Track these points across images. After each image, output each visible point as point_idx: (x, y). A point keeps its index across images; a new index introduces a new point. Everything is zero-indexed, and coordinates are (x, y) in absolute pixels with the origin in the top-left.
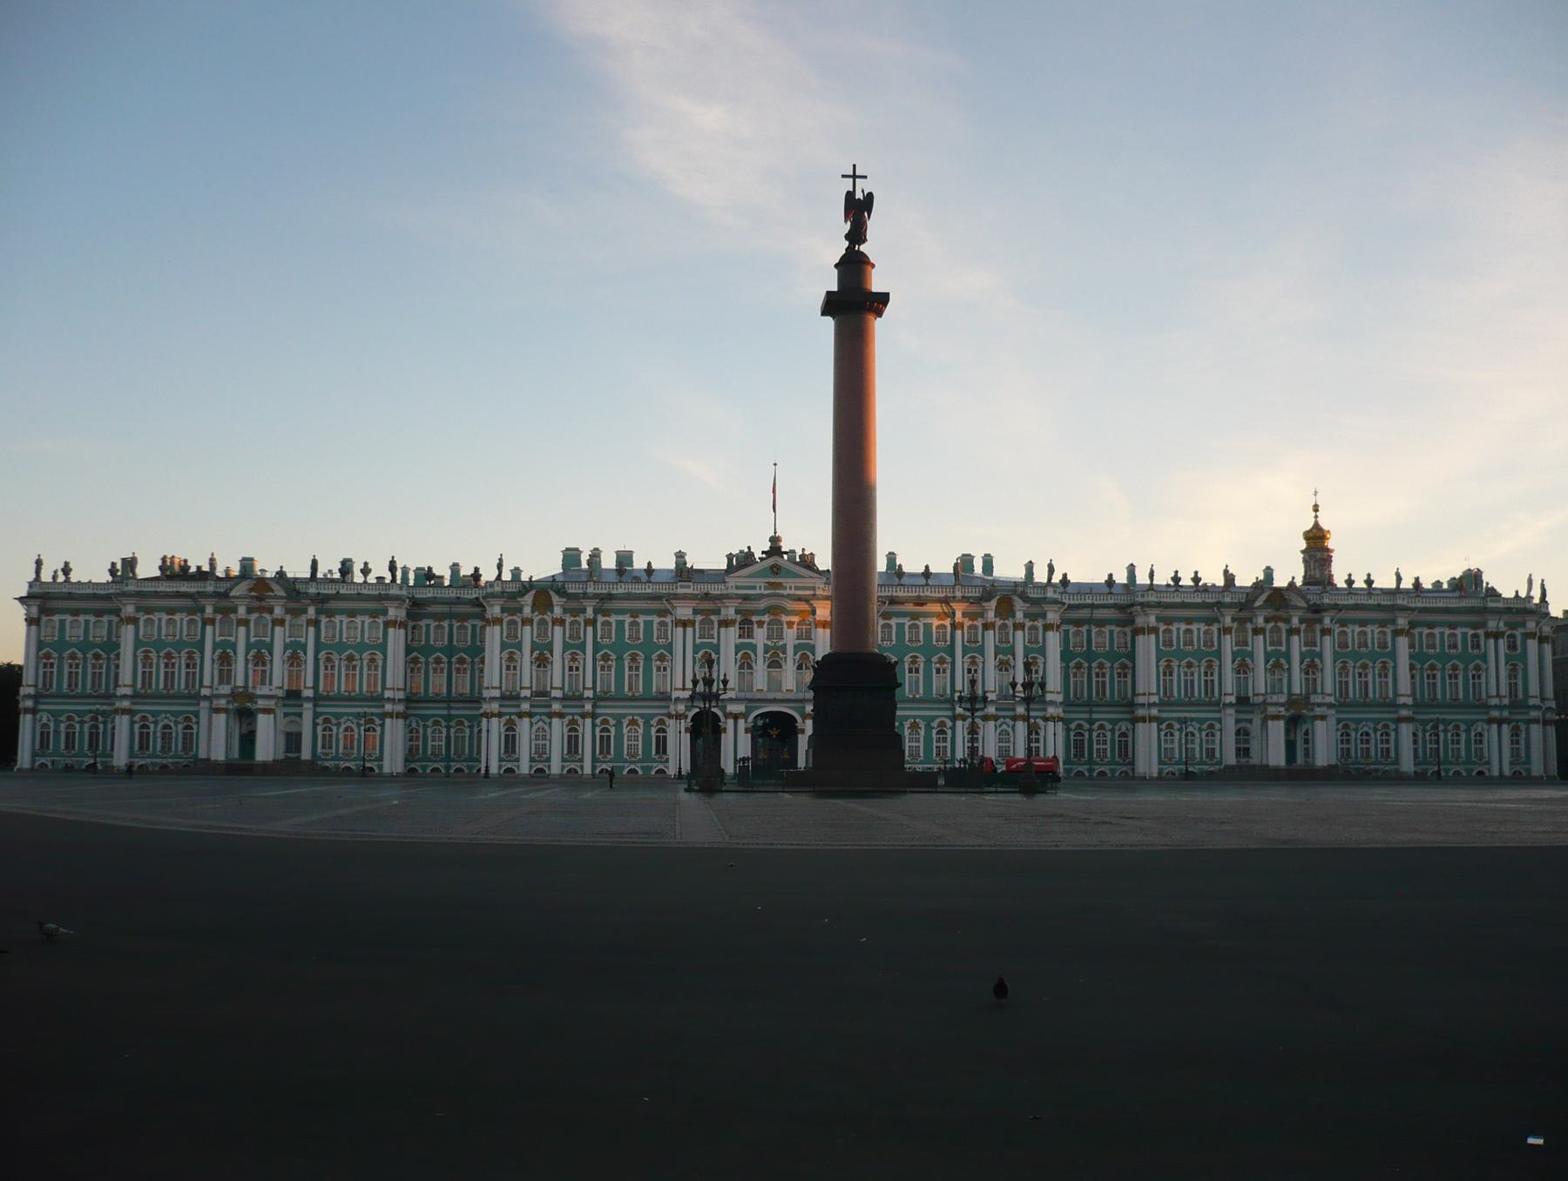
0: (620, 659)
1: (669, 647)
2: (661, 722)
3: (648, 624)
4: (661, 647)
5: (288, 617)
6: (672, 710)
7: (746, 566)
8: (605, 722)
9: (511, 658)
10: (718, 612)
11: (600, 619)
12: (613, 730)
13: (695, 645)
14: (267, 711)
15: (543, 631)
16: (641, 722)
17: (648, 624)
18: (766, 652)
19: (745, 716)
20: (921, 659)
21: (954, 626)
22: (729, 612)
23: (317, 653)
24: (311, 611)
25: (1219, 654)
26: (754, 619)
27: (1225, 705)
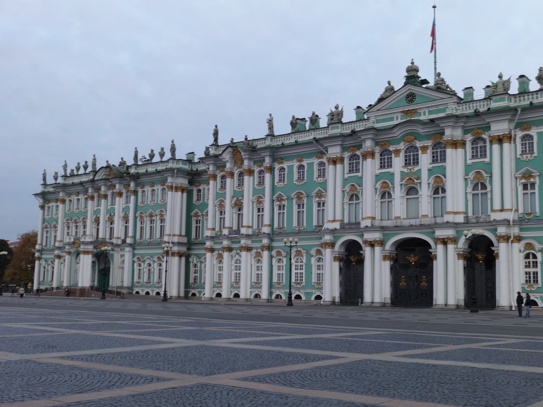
0: (289, 199)
1: (324, 185)
2: (319, 252)
4: (320, 184)
5: (124, 191)
8: (279, 253)
10: (359, 147)
11: (277, 166)
12: (284, 260)
14: (86, 252)
16: (303, 251)
17: (311, 165)
18: (402, 180)
19: (382, 243)
22: (368, 145)
23: (135, 212)
24: (132, 184)
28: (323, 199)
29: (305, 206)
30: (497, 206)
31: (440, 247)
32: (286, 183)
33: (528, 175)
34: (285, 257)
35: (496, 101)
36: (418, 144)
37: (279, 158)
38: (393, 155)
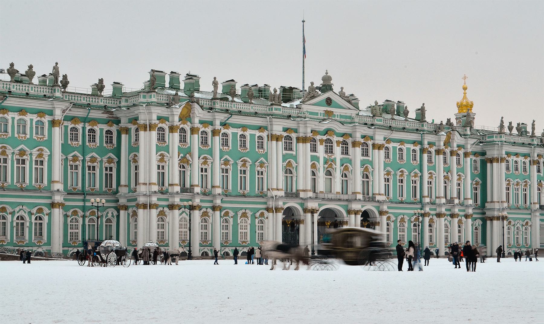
2: (262, 215)
3: (252, 136)
4: (262, 155)
6: (271, 204)
7: (313, 97)
9: (162, 159)
12: (231, 220)
13: (284, 156)
15: (183, 140)
16: (249, 213)
18: (326, 162)
20: (406, 173)
21: (422, 151)
25: (529, 177)
26: (318, 137)
27: (535, 211)
28: (263, 168)
29: (248, 173)
30: (377, 192)
31: (353, 216)
32: (231, 148)
33: (388, 173)
34: (232, 217)
35: (377, 120)
36: (335, 139)
37: (227, 123)
38: (318, 143)
